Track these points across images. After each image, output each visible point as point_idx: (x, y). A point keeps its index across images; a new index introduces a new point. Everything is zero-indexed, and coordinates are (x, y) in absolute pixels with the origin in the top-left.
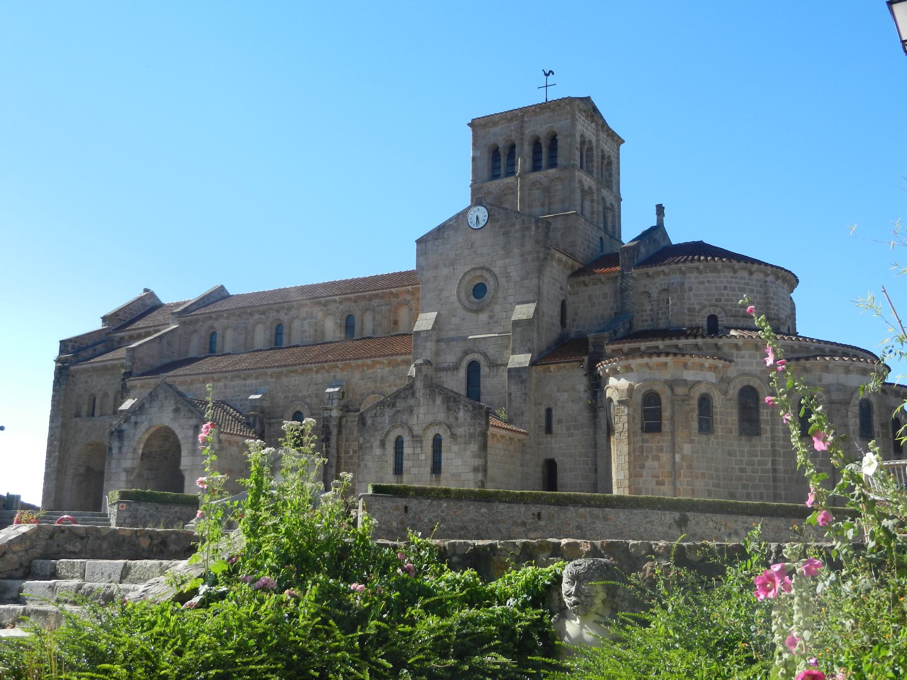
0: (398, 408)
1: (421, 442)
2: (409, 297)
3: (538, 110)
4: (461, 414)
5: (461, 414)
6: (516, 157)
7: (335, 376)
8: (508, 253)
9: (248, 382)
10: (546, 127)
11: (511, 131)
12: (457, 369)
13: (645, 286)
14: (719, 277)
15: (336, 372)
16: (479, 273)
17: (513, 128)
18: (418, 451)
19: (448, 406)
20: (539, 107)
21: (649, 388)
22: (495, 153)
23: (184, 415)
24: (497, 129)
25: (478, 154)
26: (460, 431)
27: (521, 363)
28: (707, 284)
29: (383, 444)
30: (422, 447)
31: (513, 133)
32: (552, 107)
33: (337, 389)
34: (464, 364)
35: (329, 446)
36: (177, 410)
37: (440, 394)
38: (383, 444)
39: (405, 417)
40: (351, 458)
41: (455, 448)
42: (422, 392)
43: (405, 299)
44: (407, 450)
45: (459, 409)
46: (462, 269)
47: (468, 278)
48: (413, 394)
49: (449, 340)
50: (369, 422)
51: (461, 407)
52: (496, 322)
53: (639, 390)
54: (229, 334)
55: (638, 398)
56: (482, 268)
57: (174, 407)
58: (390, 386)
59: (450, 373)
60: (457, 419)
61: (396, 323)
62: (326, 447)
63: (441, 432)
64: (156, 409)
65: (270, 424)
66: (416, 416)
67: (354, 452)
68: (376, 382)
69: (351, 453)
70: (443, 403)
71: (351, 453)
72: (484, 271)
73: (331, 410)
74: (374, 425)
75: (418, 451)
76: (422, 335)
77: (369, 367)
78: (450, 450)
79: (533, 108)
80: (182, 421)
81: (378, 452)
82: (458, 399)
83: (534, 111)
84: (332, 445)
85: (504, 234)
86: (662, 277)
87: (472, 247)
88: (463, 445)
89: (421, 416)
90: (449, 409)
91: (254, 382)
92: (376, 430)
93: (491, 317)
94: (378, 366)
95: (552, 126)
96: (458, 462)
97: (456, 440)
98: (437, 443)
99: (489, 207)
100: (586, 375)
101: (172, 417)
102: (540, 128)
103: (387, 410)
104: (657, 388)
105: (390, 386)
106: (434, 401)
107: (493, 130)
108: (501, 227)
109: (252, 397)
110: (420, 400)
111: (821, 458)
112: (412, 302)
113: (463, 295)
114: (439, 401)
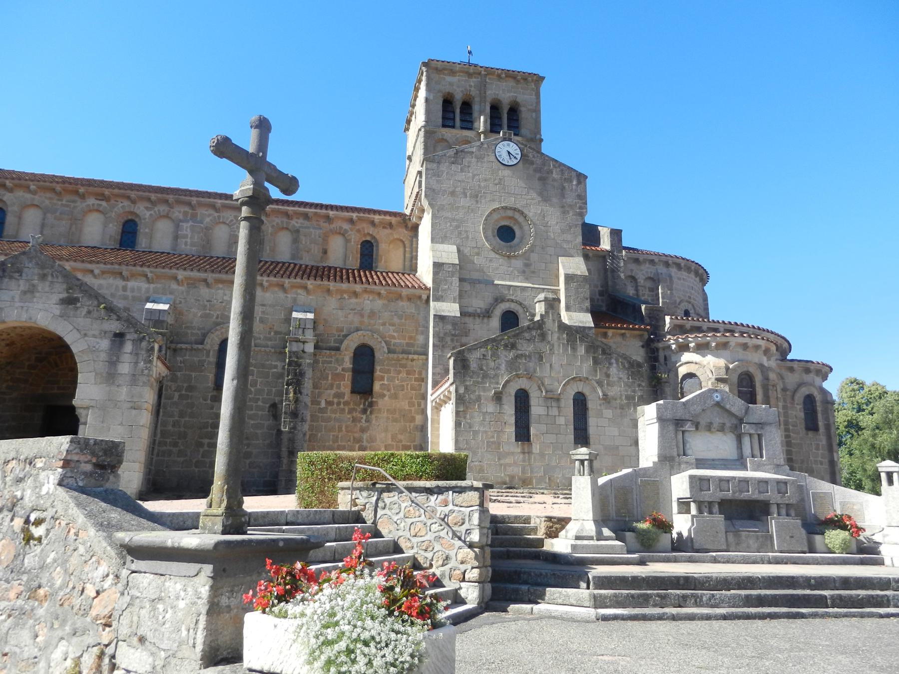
0: (520, 352)
1: (558, 400)
2: (346, 226)
3: (503, 75)
4: (613, 370)
5: (613, 370)
6: (475, 114)
7: (295, 300)
8: (545, 199)
9: (131, 284)
10: (508, 95)
11: (470, 86)
12: (489, 317)
13: (632, 270)
14: (689, 277)
15: (297, 294)
16: (510, 213)
17: (472, 84)
18: (554, 411)
19: (594, 358)
20: (505, 73)
21: (745, 369)
22: (448, 103)
23: (89, 312)
24: (454, 79)
25: (431, 97)
26: (613, 392)
27: (582, 322)
28: (682, 281)
29: (498, 397)
30: (559, 407)
31: (473, 89)
32: (519, 77)
33: (310, 316)
34: (498, 312)
35: (301, 393)
36: (70, 301)
37: (581, 340)
38: (498, 397)
39: (531, 364)
40: (322, 411)
41: (608, 413)
42: (556, 336)
43: (341, 228)
44: (537, 409)
45: (610, 364)
46: (487, 208)
47: (496, 216)
48: (543, 336)
49: (474, 282)
50: (473, 365)
51: (613, 361)
52: (533, 272)
53: (734, 369)
54: (32, 217)
55: (735, 379)
56: (515, 209)
57: (65, 295)
58: (384, 324)
59: (478, 320)
60: (608, 376)
61: (325, 252)
62: (295, 393)
63: (587, 391)
64: (17, 294)
65: (175, 350)
66: (548, 365)
67: (329, 403)
68: (362, 316)
69: (323, 405)
70: (587, 351)
71: (323, 405)
72: (516, 213)
73: (304, 342)
74: (482, 369)
75: (554, 411)
76: (446, 268)
77: (355, 294)
78: (600, 415)
79: (500, 72)
80: (82, 321)
81: (491, 408)
82: (608, 351)
83: (499, 76)
84: (304, 391)
85: (540, 179)
86: (647, 265)
87: (500, 183)
88: (619, 411)
89: (556, 366)
90: (596, 362)
91: (144, 285)
92: (485, 376)
93: (527, 265)
94: (366, 296)
95: (516, 97)
96: (614, 431)
97: (609, 402)
98: (580, 403)
99: (520, 145)
100: (643, 346)
101: (58, 312)
102: (505, 93)
103: (502, 352)
104: (752, 370)
105: (384, 324)
106: (574, 349)
107: (449, 79)
108: (535, 170)
109: (149, 306)
110: (553, 346)
111: (821, 451)
112: (350, 233)
113: (490, 233)
114: (581, 350)
